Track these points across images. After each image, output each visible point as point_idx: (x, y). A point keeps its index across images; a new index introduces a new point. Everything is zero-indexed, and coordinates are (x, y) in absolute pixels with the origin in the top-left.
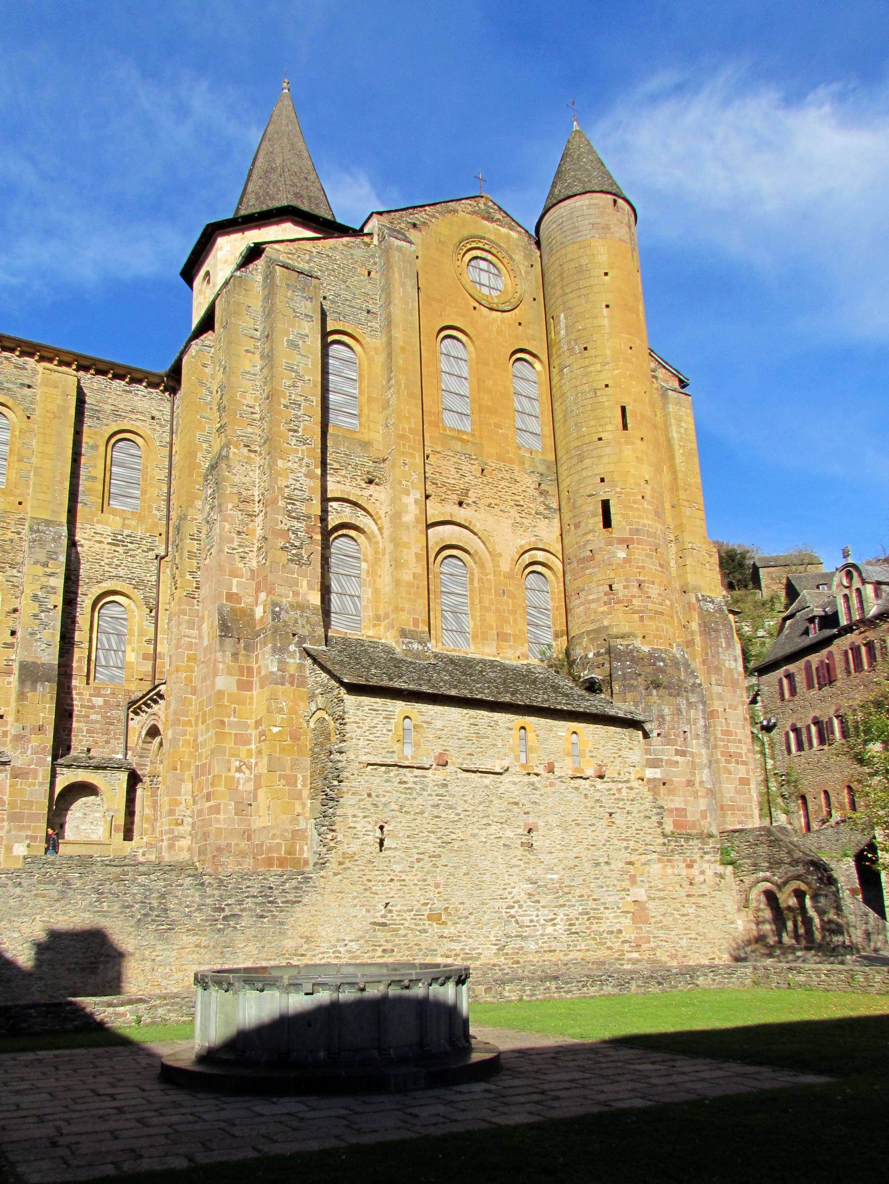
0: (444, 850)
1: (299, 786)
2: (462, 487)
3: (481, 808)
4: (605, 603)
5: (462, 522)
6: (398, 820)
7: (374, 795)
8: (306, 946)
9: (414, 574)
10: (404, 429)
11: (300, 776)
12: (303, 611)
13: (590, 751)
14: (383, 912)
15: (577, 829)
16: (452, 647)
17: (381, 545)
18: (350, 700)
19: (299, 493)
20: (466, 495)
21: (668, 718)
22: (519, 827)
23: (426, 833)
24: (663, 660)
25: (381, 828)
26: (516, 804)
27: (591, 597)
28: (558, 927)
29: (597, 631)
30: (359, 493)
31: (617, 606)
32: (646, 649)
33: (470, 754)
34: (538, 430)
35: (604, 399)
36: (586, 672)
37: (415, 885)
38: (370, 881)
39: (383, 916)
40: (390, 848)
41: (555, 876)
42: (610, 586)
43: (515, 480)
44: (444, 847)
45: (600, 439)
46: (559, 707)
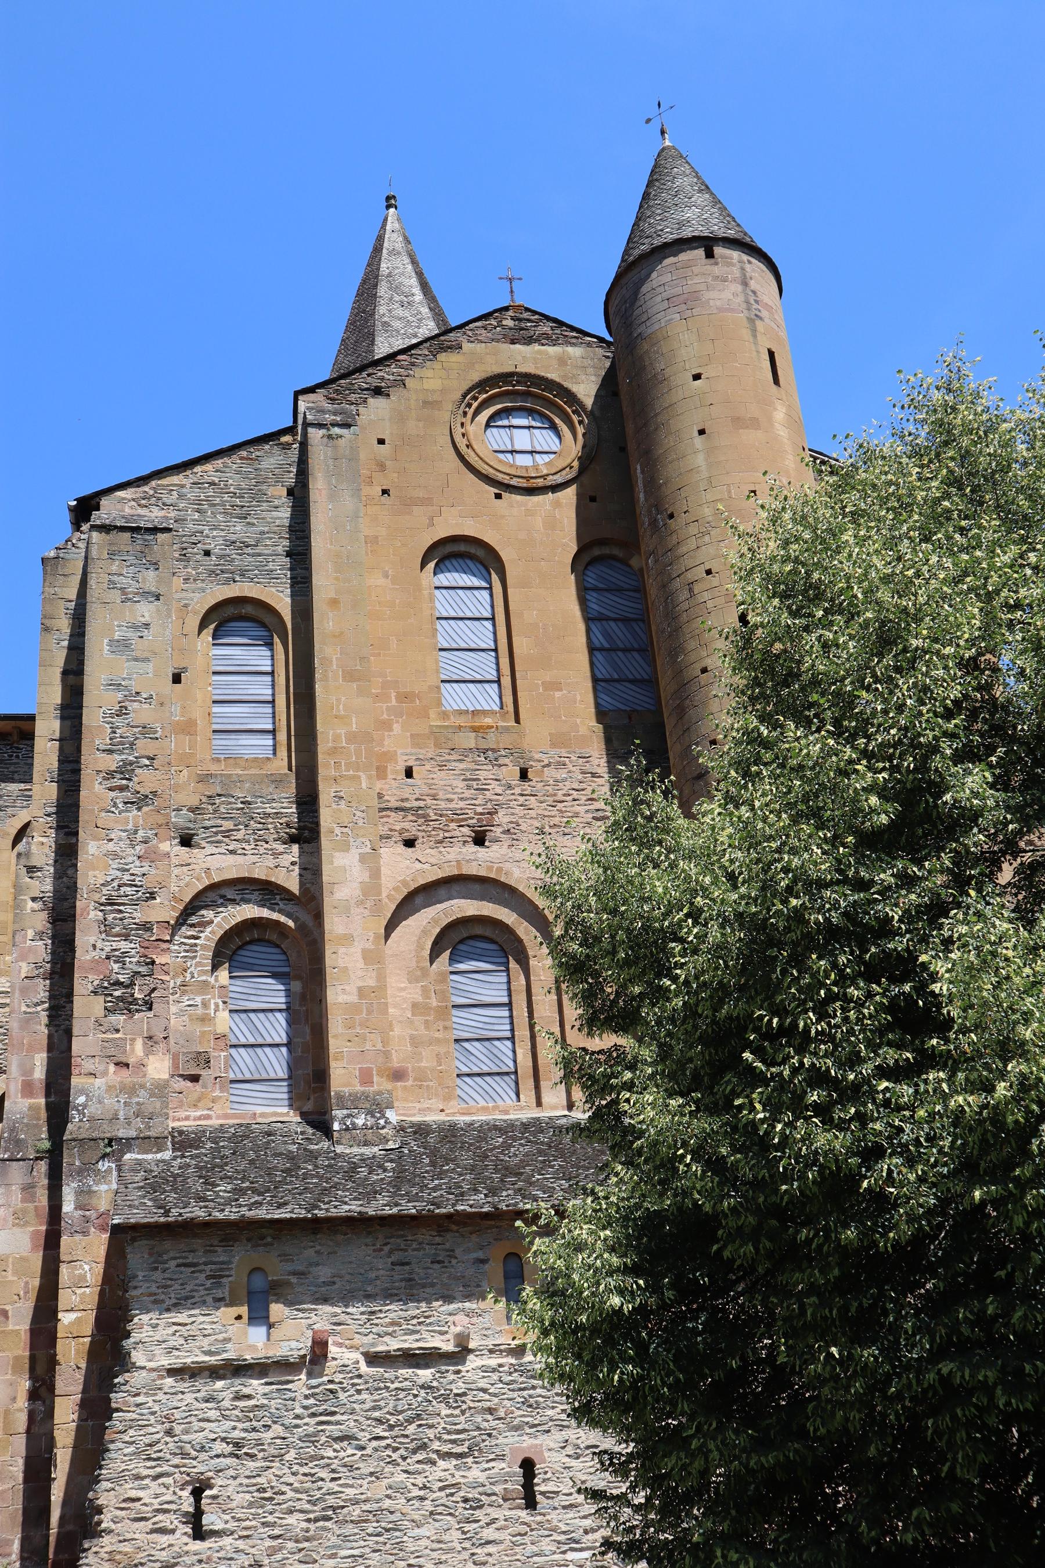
2: (480, 810)
3: (411, 1429)
5: (483, 873)
6: (231, 1472)
7: (178, 1429)
9: (360, 990)
16: (482, 1103)
19: (128, 890)
22: (501, 1458)
23: (290, 1494)
26: (490, 1411)
33: (393, 1323)
35: (706, 596)
44: (328, 1519)
45: (704, 670)
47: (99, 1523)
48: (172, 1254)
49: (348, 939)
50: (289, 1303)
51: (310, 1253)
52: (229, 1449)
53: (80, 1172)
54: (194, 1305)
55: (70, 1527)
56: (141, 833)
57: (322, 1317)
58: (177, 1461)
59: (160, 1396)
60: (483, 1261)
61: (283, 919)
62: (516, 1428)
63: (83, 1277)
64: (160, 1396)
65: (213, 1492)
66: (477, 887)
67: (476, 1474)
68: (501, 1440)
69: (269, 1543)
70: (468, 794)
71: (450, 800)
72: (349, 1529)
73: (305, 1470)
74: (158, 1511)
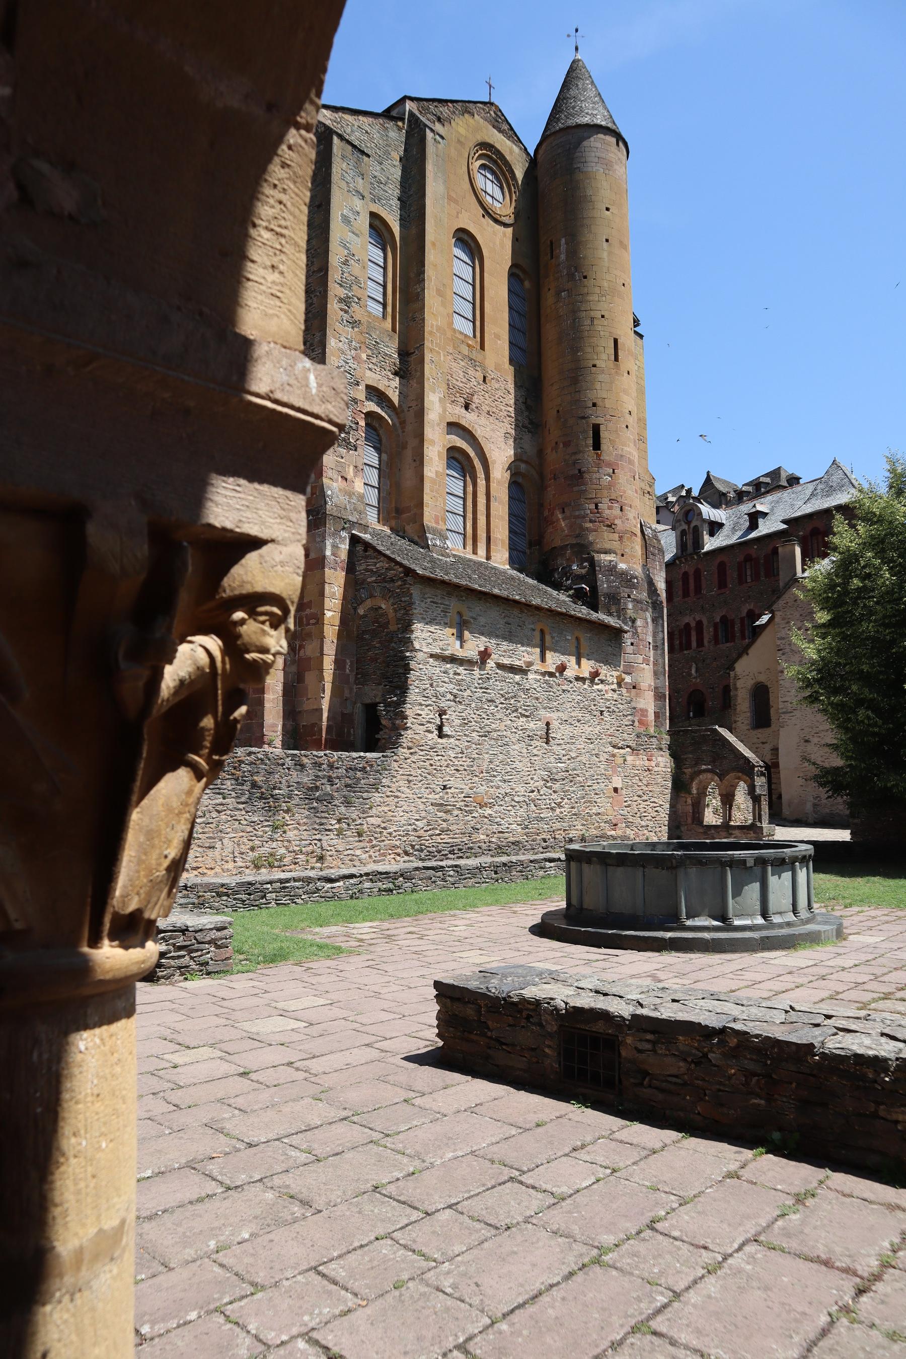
3: (512, 701)
7: (435, 684)
9: (437, 472)
10: (432, 326)
11: (348, 661)
15: (577, 724)
22: (540, 720)
23: (474, 723)
24: (636, 578)
25: (440, 715)
26: (537, 699)
28: (563, 810)
32: (622, 566)
33: (505, 651)
36: (569, 582)
37: (465, 770)
38: (431, 765)
39: (442, 798)
40: (448, 736)
44: (486, 736)
45: (594, 366)
46: (573, 613)
47: (406, 724)
48: (429, 595)
49: (433, 442)
50: (471, 633)
51: (477, 609)
52: (452, 698)
53: (333, 534)
54: (437, 624)
55: (331, 723)
56: (354, 344)
57: (491, 643)
58: (434, 699)
59: (428, 667)
60: (534, 630)
61: (386, 417)
62: (545, 708)
63: (334, 593)
65: (447, 717)
66: (461, 432)
67: (532, 725)
70: (464, 380)
72: (493, 742)
73: (478, 713)
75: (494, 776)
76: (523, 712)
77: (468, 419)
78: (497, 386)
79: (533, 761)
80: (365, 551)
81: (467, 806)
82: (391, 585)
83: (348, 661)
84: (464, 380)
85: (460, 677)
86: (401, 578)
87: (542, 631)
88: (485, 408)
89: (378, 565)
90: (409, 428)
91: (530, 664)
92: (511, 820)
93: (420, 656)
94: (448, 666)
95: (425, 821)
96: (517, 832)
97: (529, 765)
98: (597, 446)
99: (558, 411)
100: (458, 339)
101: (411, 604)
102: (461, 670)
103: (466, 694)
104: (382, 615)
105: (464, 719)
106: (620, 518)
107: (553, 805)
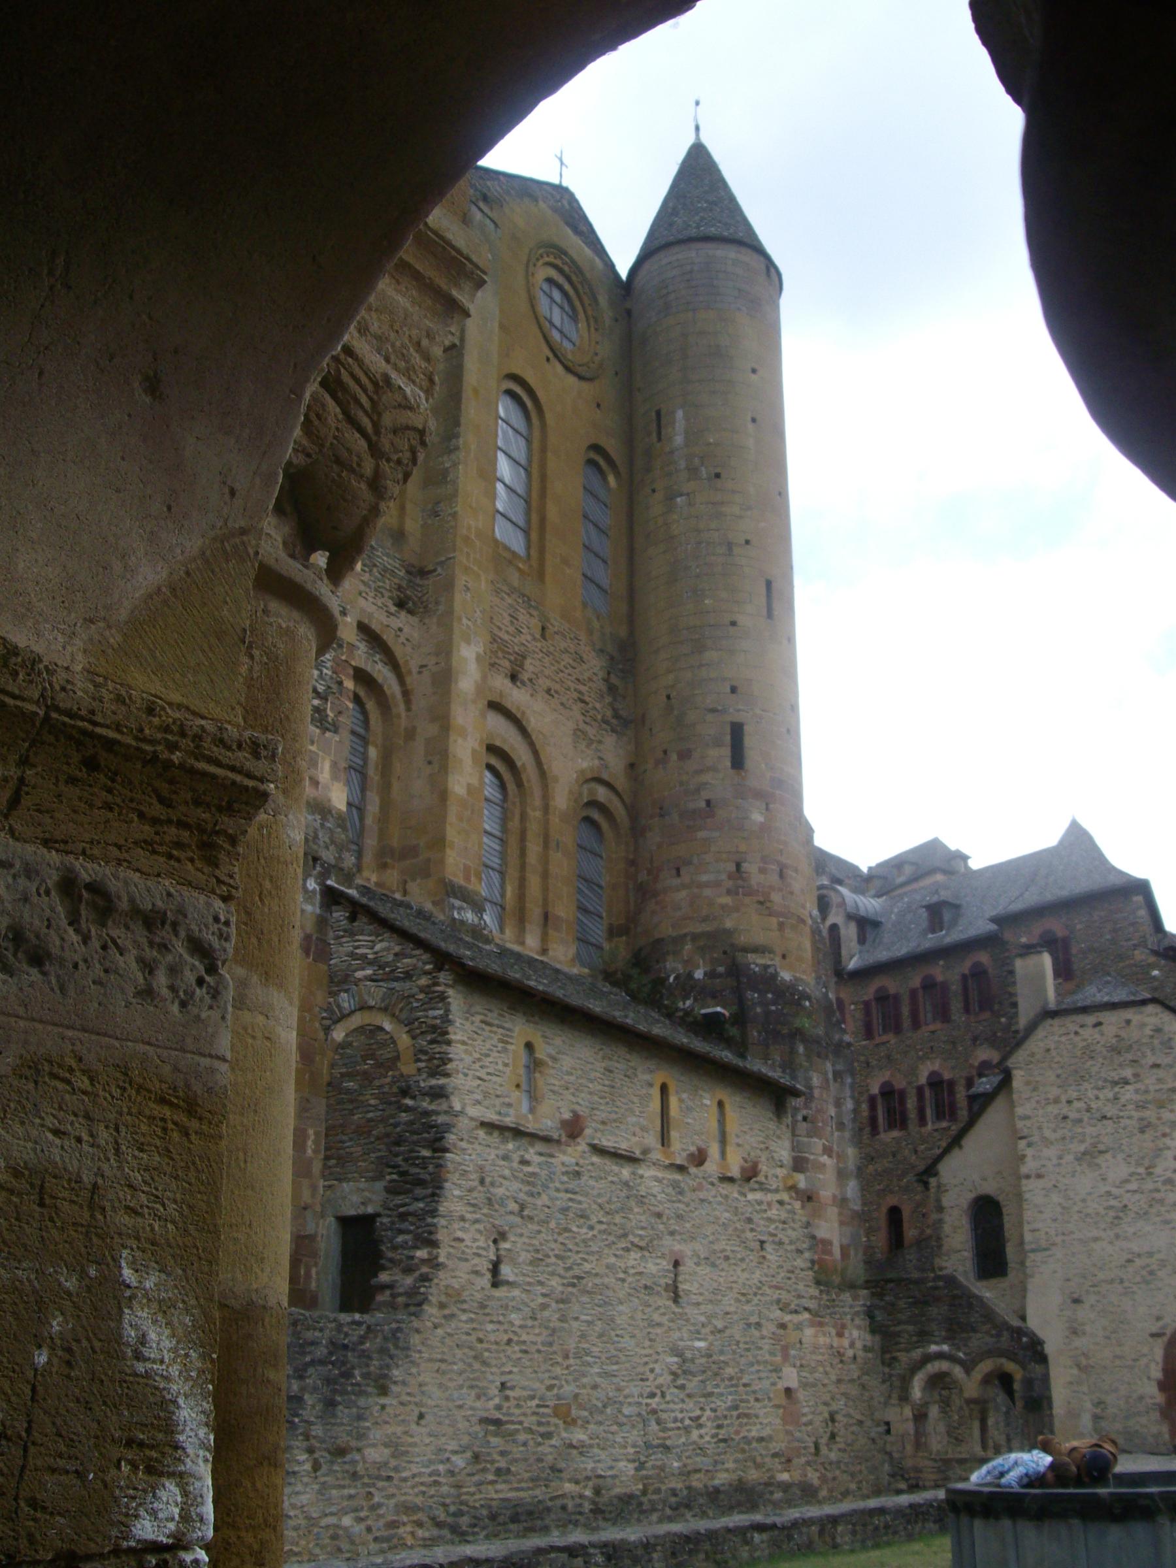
0: (574, 1290)
1: (309, 1151)
2: (516, 649)
4: (729, 892)
7: (488, 1180)
8: (393, 1463)
9: (469, 784)
11: (311, 1132)
12: (324, 819)
13: (737, 1136)
14: (497, 1401)
15: (725, 1265)
17: (403, 722)
18: (456, 1000)
20: (521, 666)
21: (816, 1093)
22: (663, 1256)
24: (809, 998)
26: (659, 1215)
27: (704, 878)
29: (713, 936)
30: (385, 621)
31: (747, 900)
33: (603, 1123)
34: (605, 582)
36: (688, 1003)
37: (539, 1351)
38: (480, 1341)
39: (498, 1408)
40: (508, 1283)
41: (701, 1344)
42: (738, 865)
43: (581, 658)
44: (574, 1285)
45: (733, 624)
49: (463, 733)
60: (651, 1085)
64: (476, 1146)
68: (664, 1242)
69: (541, 1300)
71: (500, 629)
73: (560, 1239)
74: (475, 1254)
75: (589, 1364)
76: (636, 1240)
77: (517, 697)
78: (563, 645)
79: (652, 1336)
80: (353, 918)
81: (540, 1424)
82: (408, 984)
83: (311, 1132)
84: (511, 629)
85: (530, 1169)
86: (426, 973)
87: (664, 1089)
88: (544, 683)
89: (378, 947)
90: (420, 703)
91: (646, 1152)
92: (617, 1451)
93: (463, 1123)
94: (510, 1146)
95: (469, 1454)
96: (623, 1474)
97: (647, 1343)
98: (738, 760)
99: (668, 697)
100: (501, 557)
101: (446, 1019)
102: (531, 1154)
103: (539, 1202)
104: (383, 1045)
105: (537, 1251)
106: (781, 890)
107: (687, 1422)
